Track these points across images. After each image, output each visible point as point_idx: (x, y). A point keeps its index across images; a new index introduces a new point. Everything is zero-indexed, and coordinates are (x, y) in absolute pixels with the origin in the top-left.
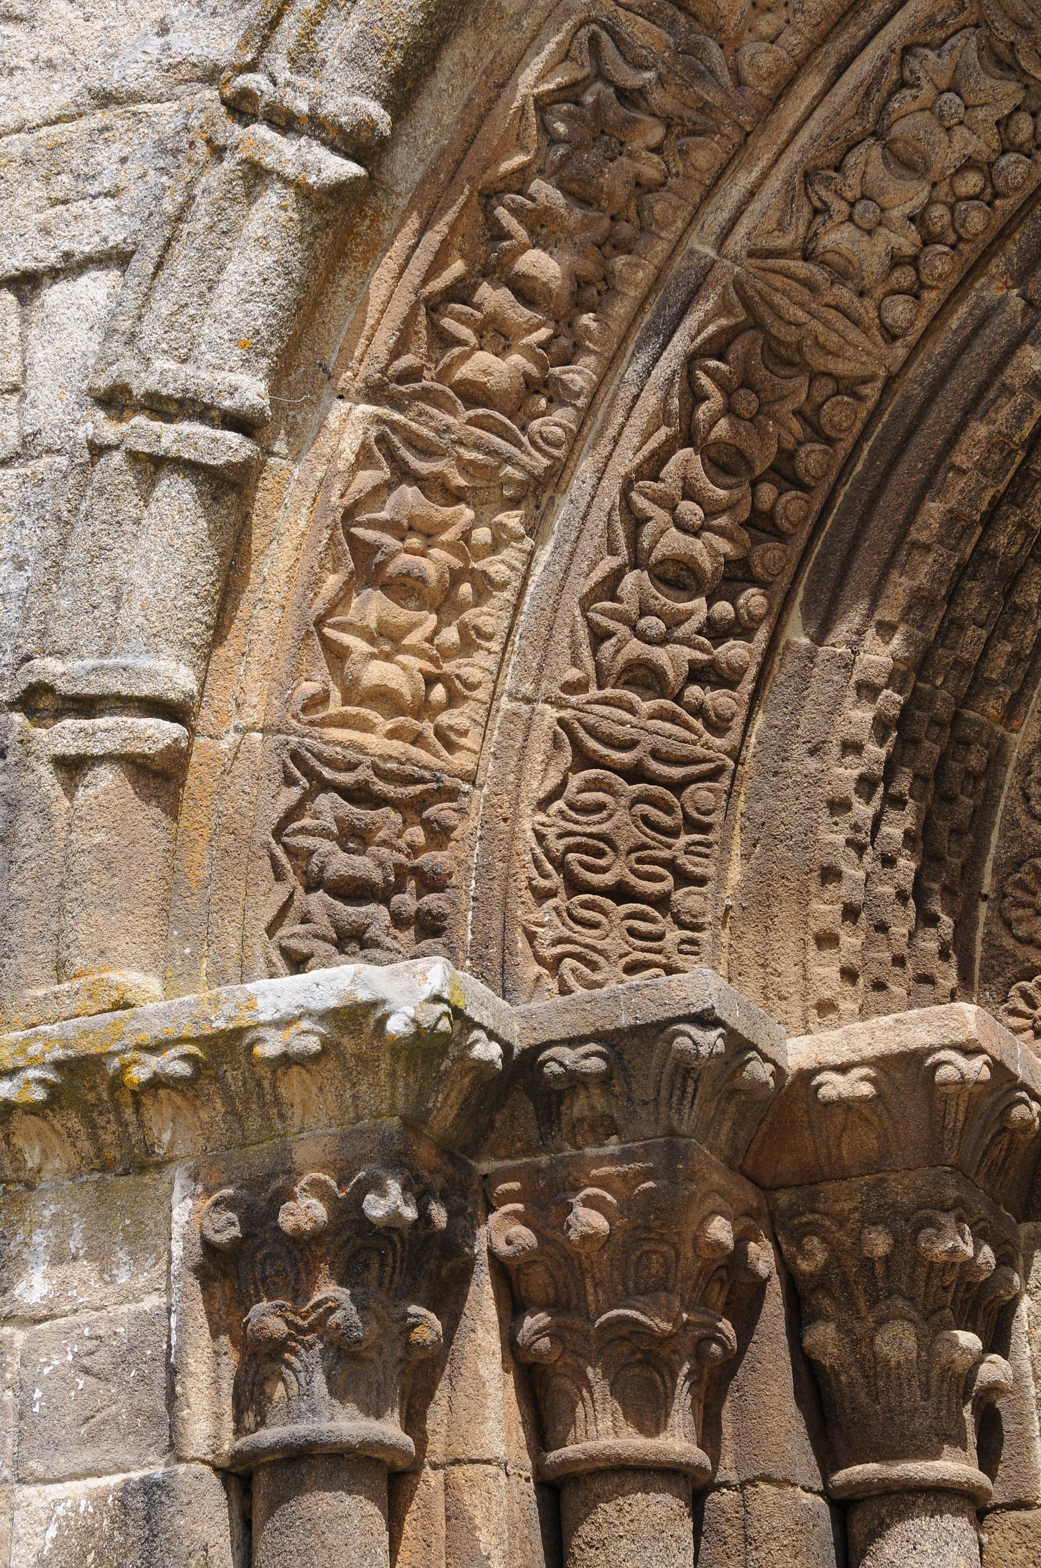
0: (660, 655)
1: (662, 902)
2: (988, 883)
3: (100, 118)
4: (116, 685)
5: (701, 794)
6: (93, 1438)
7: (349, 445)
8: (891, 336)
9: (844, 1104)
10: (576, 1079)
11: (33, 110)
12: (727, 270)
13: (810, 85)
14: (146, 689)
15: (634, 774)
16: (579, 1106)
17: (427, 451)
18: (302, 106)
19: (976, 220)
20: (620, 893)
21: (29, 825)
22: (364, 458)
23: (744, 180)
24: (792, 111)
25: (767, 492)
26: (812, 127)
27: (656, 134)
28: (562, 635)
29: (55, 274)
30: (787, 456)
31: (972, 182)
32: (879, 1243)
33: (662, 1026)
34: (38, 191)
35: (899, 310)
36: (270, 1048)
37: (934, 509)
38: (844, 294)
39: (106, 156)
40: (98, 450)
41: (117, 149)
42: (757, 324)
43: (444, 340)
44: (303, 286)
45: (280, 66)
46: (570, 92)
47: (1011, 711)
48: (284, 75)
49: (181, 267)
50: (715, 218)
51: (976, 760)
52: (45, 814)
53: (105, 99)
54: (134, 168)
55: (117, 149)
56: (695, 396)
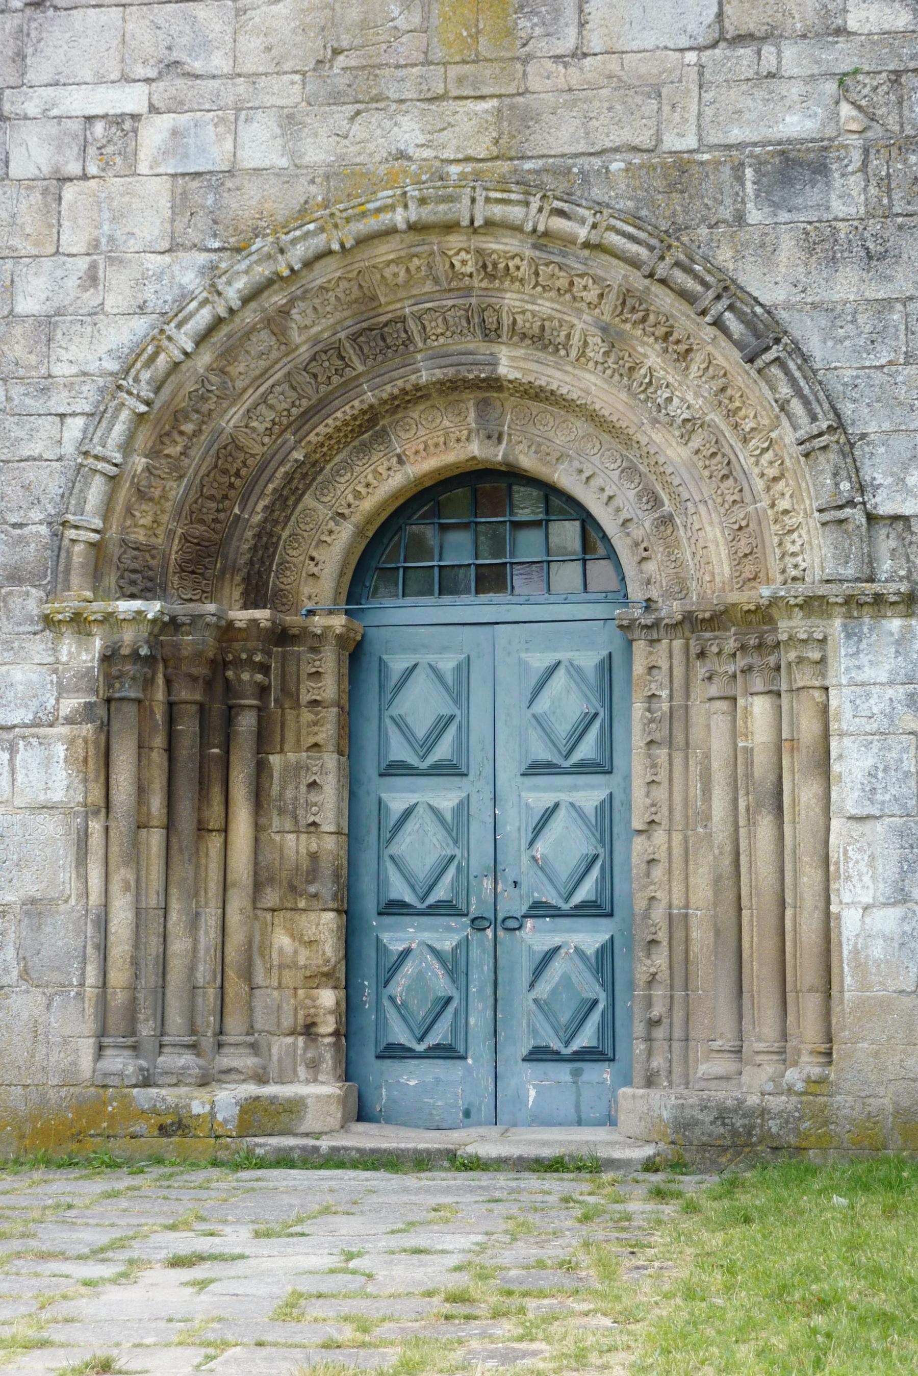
0: (205, 517)
1: (202, 574)
2: (274, 568)
3: (82, 379)
4: (85, 524)
5: (213, 549)
6: (77, 691)
7: (139, 469)
8: (263, 445)
9: (240, 629)
10: (184, 624)
11: (67, 373)
12: (229, 430)
13: (251, 391)
14: (93, 527)
15: (198, 544)
16: (184, 629)
17: (156, 468)
18: (135, 392)
19: (285, 422)
20: (193, 572)
21: (63, 554)
22: (143, 471)
23: (234, 410)
24: (246, 396)
25: (233, 479)
26: (250, 401)
27: (215, 399)
28: (184, 513)
29: (70, 415)
30: (238, 470)
31: (285, 413)
32: (244, 656)
33: (203, 615)
34: (66, 394)
35: (266, 440)
36: (121, 617)
37: (271, 486)
38: (254, 436)
39: (85, 388)
40: (81, 465)
41: (87, 388)
42: (234, 441)
43: (162, 443)
44: (129, 429)
45: (130, 381)
46: (197, 391)
47: (283, 529)
48: (131, 383)
49: (104, 423)
50: (227, 418)
51: (274, 540)
52: (68, 552)
53: (85, 374)
54: (91, 393)
55: (87, 388)
56: (219, 458)
